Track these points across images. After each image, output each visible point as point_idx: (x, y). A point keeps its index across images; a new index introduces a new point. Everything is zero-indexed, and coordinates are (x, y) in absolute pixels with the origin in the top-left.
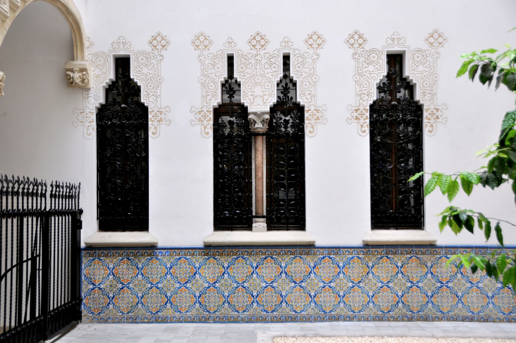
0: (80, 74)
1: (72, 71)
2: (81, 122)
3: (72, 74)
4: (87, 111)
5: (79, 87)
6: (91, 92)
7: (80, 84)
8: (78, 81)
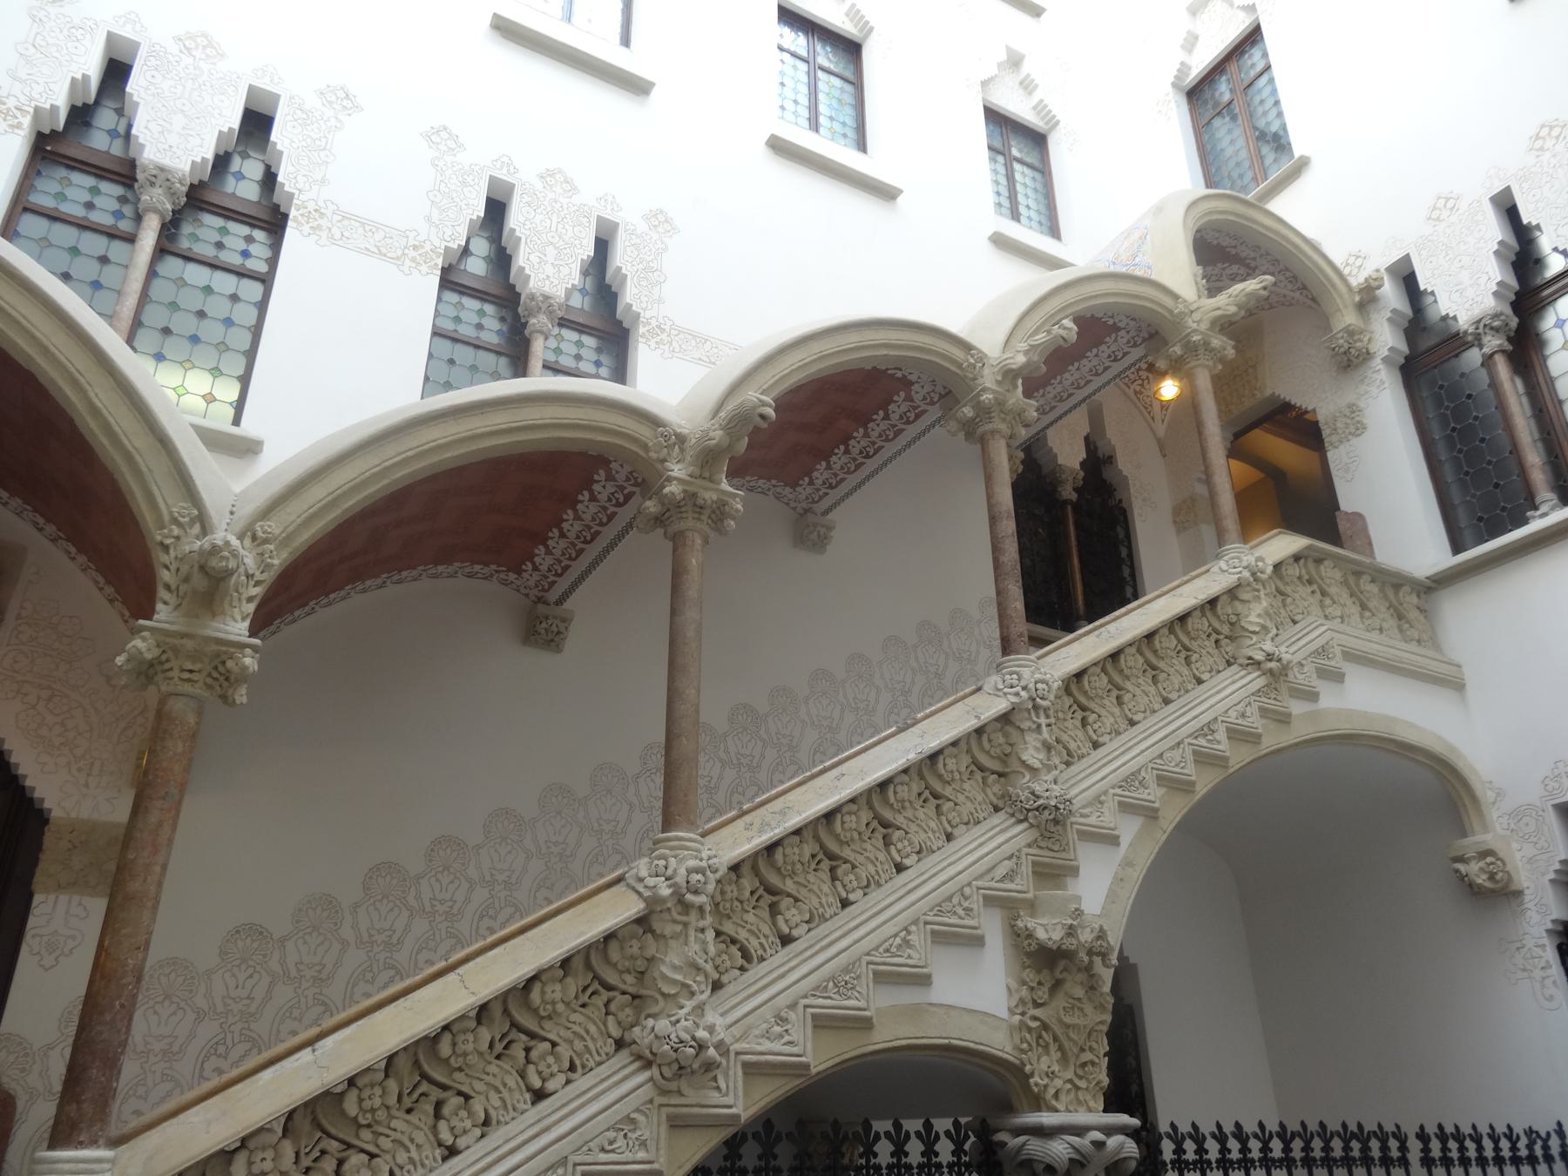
0: (1482, 864)
1: (1461, 859)
2: (1524, 970)
3: (1462, 867)
4: (1529, 942)
5: (1493, 891)
6: (1527, 898)
7: (1488, 884)
8: (1481, 880)
